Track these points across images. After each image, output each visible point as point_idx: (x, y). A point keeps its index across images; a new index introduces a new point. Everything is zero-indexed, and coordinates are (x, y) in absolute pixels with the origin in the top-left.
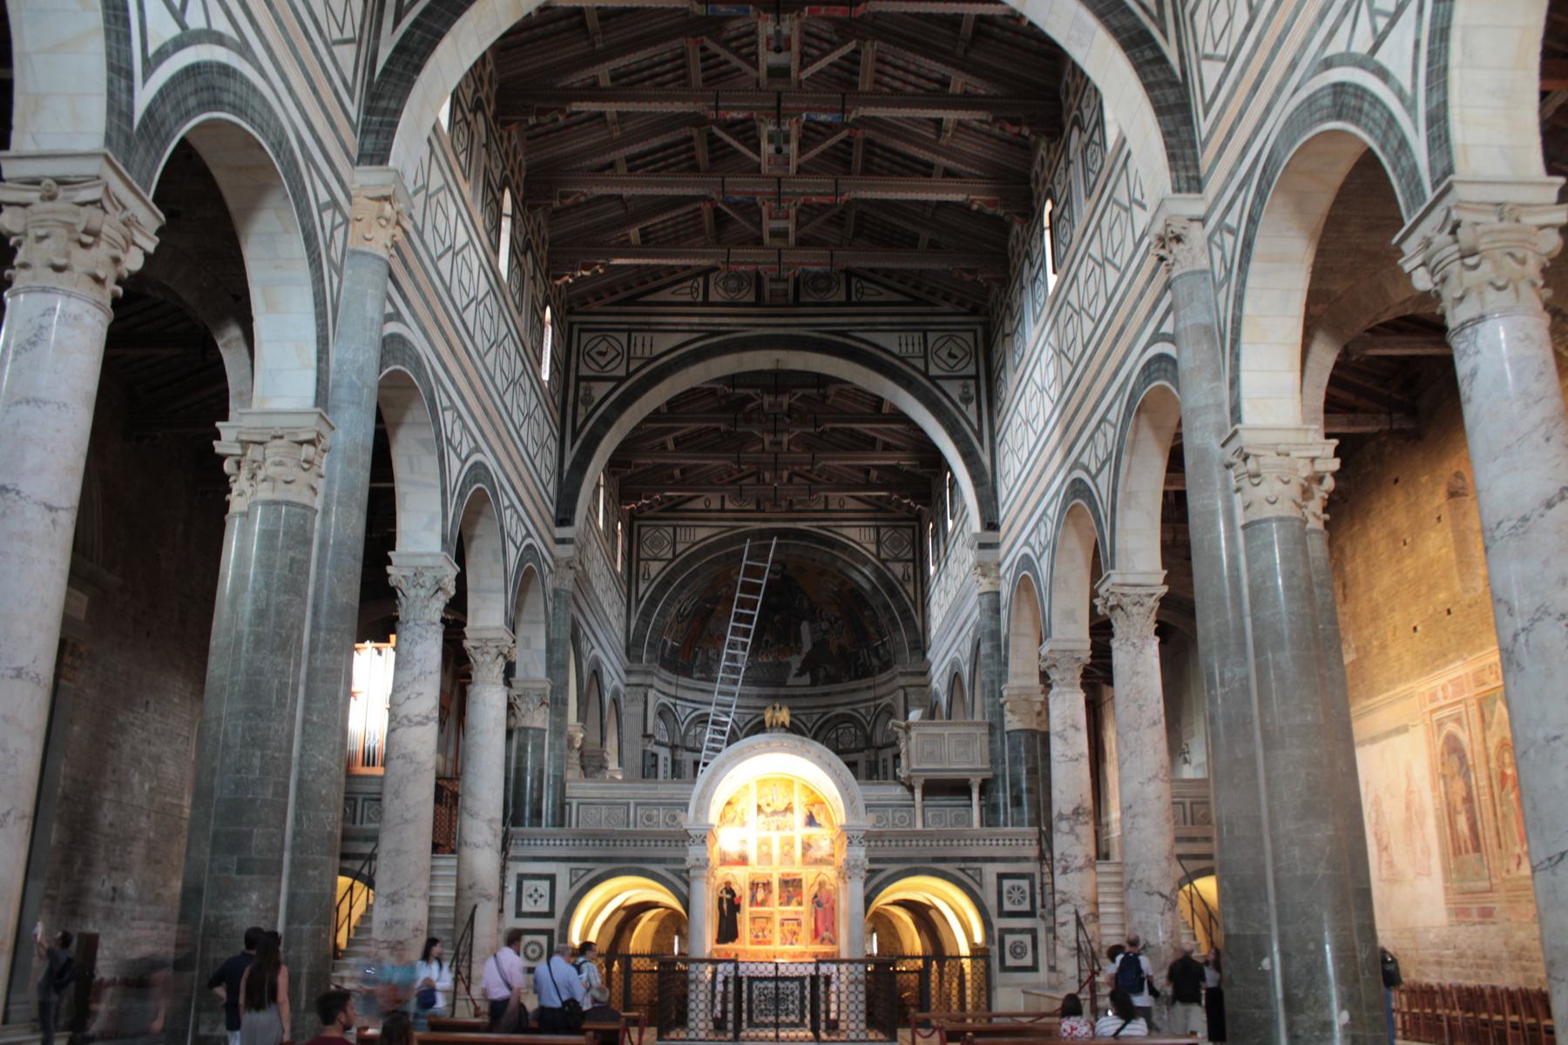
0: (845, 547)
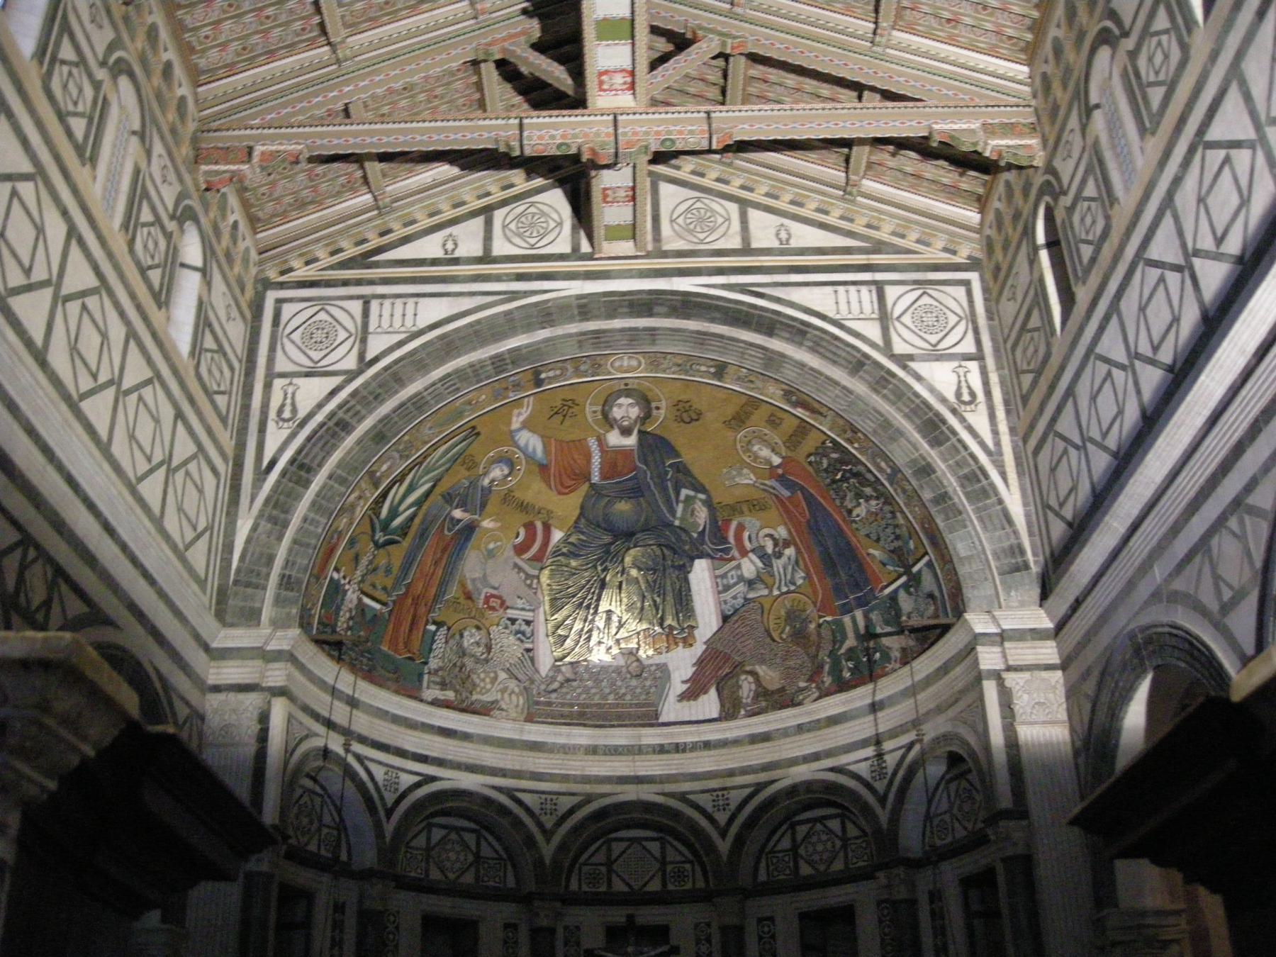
0: (798, 332)
